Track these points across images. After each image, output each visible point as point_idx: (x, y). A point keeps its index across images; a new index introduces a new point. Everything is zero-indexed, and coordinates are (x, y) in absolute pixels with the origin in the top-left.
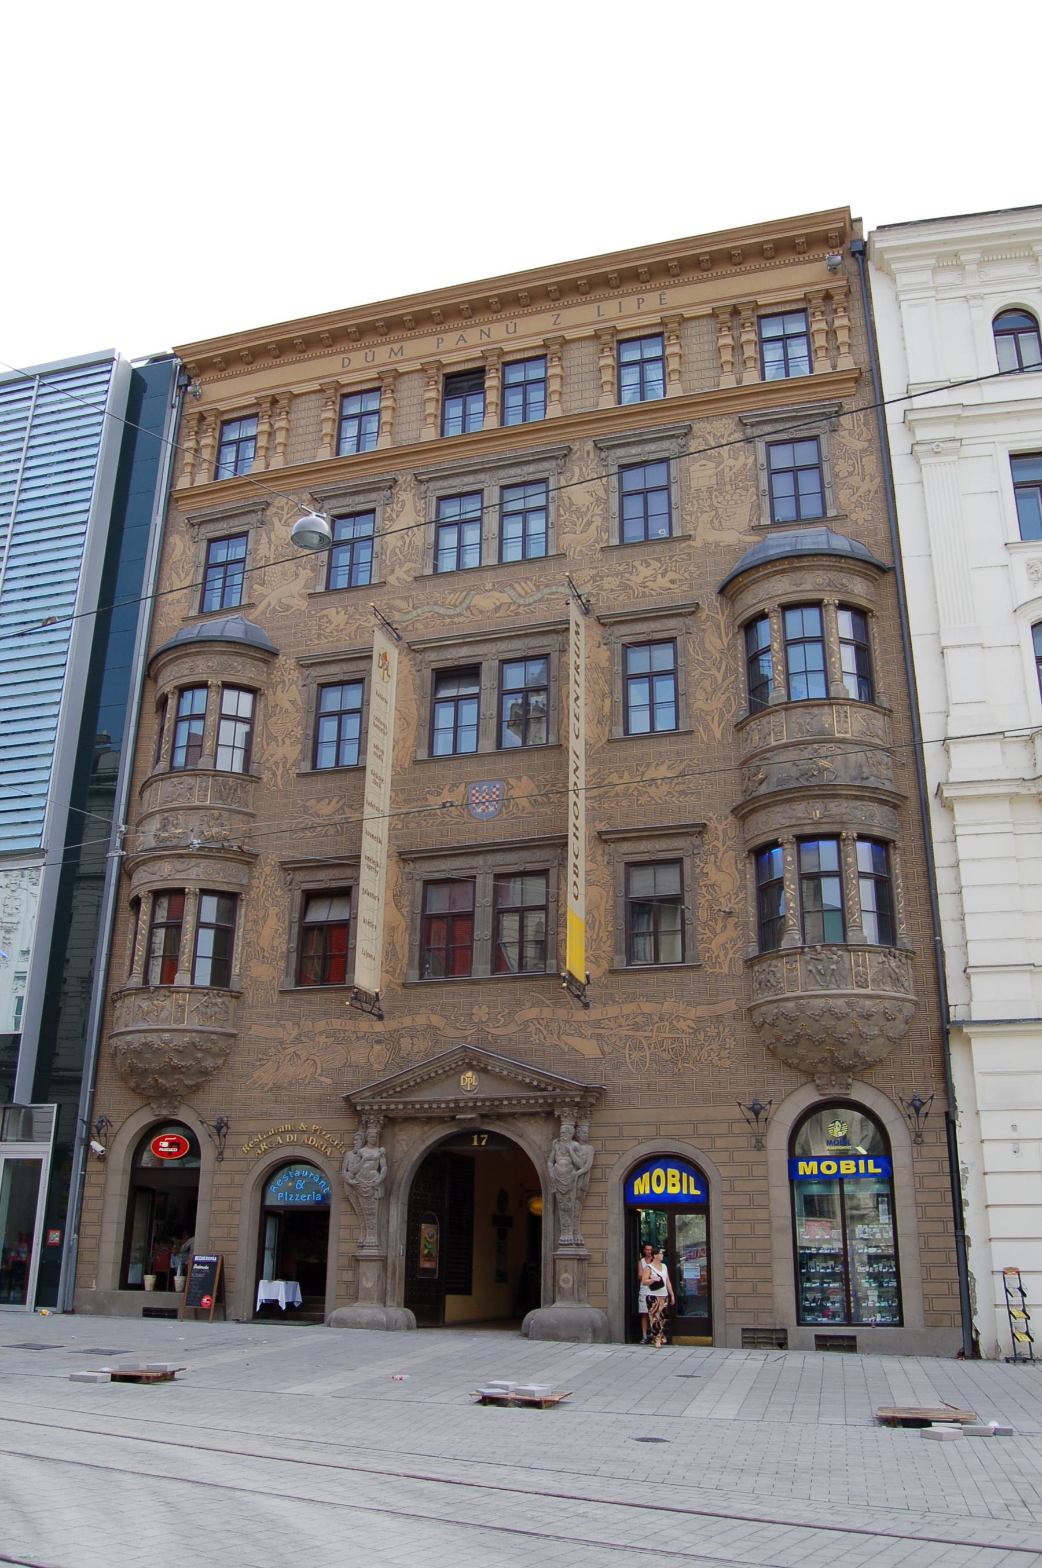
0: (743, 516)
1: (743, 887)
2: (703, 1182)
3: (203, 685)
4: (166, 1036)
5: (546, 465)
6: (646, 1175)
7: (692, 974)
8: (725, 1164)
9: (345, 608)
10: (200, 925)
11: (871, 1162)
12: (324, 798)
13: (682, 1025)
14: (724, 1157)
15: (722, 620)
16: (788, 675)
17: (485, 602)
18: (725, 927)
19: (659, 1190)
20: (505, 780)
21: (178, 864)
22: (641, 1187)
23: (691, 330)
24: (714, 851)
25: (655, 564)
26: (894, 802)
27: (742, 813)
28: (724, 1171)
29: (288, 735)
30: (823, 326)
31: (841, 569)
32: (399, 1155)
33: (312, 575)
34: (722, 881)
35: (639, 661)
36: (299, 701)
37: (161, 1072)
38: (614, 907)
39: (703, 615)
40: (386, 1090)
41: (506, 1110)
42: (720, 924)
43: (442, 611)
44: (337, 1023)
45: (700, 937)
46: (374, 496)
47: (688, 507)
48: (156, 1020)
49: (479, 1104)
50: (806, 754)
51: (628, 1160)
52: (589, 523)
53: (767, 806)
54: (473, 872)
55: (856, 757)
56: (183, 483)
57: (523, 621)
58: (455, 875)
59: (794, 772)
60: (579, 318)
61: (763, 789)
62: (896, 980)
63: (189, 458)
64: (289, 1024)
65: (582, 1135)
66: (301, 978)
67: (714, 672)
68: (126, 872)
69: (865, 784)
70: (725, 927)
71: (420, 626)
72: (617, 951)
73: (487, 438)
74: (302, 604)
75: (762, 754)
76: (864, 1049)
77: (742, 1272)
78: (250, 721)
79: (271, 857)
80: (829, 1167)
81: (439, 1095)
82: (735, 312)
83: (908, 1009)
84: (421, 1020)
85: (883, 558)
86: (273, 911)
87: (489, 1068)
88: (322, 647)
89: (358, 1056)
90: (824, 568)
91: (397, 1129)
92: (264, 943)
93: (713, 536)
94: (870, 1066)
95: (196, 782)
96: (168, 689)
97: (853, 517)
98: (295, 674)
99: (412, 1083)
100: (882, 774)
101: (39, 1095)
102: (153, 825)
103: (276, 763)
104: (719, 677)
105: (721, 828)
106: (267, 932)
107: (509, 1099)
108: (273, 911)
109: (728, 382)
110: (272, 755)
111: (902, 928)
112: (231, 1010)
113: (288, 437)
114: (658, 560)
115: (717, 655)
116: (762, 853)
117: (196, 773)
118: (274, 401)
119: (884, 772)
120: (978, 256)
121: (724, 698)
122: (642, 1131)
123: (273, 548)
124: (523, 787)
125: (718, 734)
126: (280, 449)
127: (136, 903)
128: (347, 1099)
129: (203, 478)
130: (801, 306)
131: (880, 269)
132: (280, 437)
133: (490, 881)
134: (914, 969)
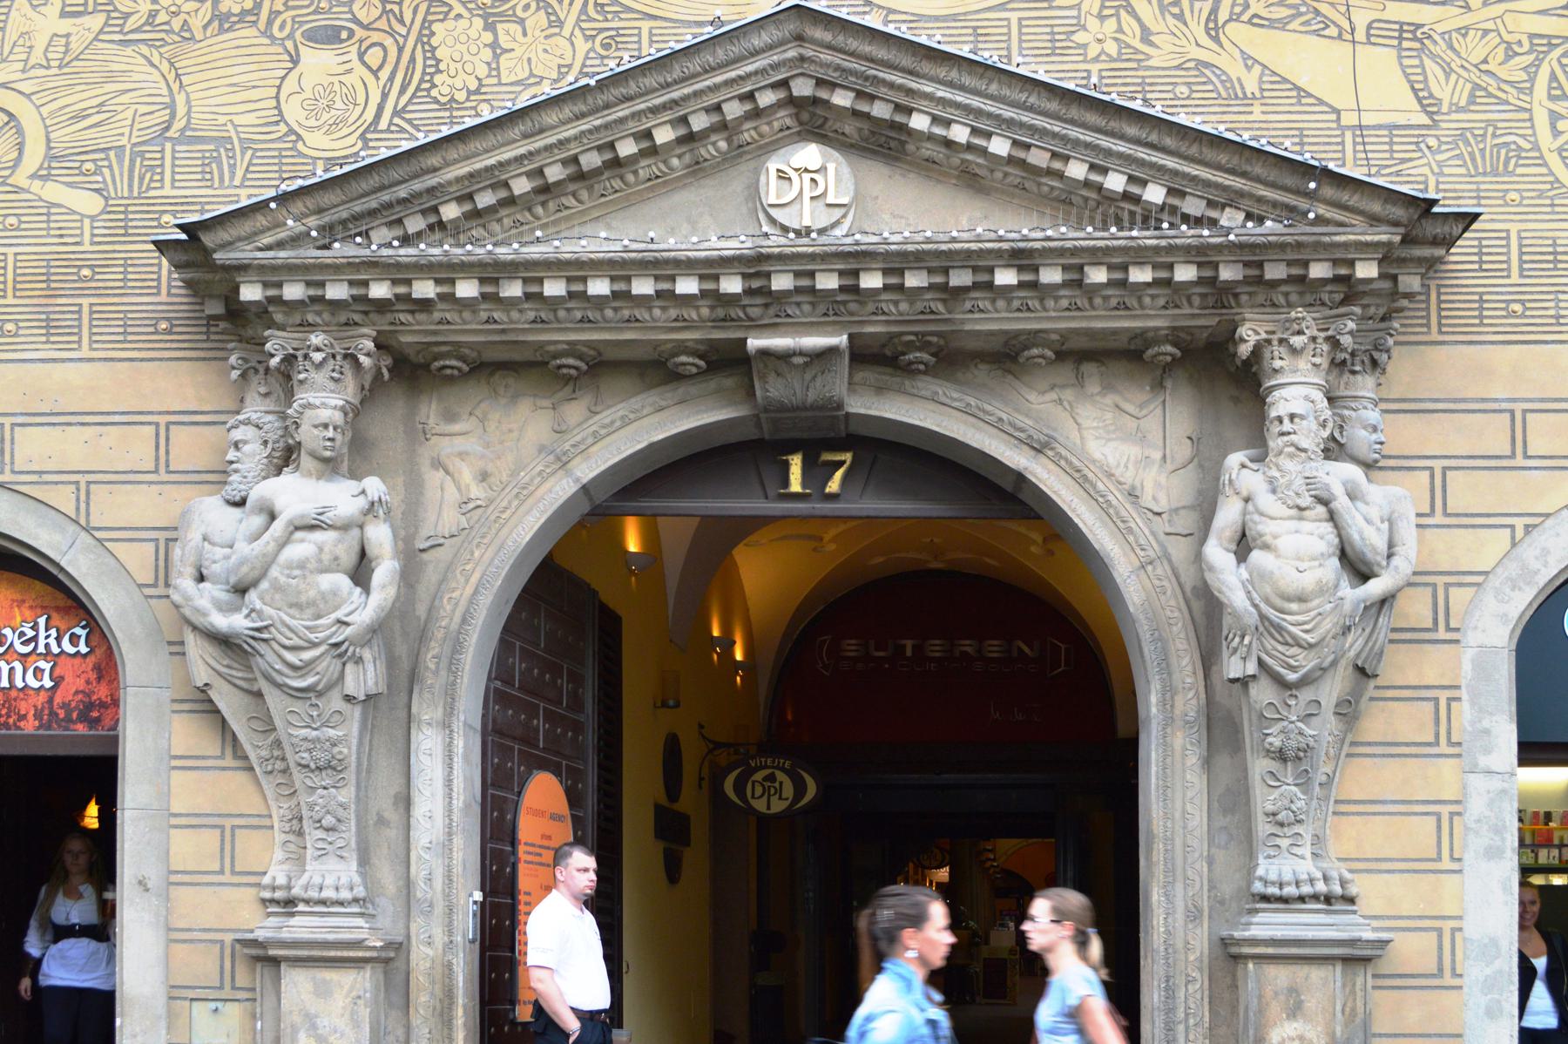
49: (872, 281)
87: (919, 122)
91: (430, 411)
99: (521, 186)
107: (1022, 258)
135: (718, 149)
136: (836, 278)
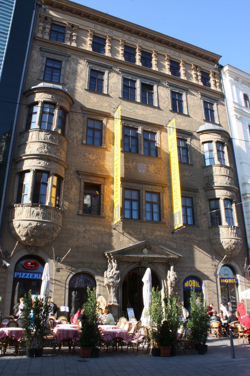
10: (53, 186)
12: (91, 154)
18: (204, 217)
24: (200, 197)
33: (85, 83)
36: (81, 120)
42: (202, 217)
44: (98, 228)
45: (198, 219)
64: (81, 226)
70: (204, 217)
103: (73, 138)
108: (74, 187)
110: (72, 135)
123: (71, 70)
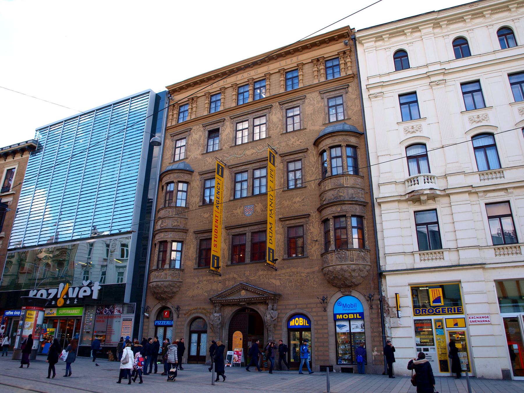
0: (320, 121)
1: (320, 233)
2: (309, 322)
3: (172, 182)
4: (162, 283)
5: (266, 111)
6: (293, 320)
7: (306, 259)
8: (315, 316)
9: (211, 157)
11: (358, 315)
13: (303, 275)
14: (315, 314)
15: (315, 152)
16: (331, 168)
17: (248, 152)
19: (297, 324)
20: (254, 205)
21: (166, 234)
22: (292, 323)
23: (306, 67)
25: (296, 138)
26: (364, 205)
27: (320, 210)
28: (315, 318)
29: (196, 195)
30: (343, 62)
31: (346, 135)
32: (225, 315)
34: (314, 230)
35: (292, 166)
37: (161, 293)
38: (284, 240)
39: (309, 152)
40: (221, 296)
41: (254, 301)
43: (237, 156)
44: (209, 278)
46: (219, 124)
47: (305, 120)
48: (158, 279)
50: (336, 191)
51: (288, 315)
52: (277, 127)
53: (325, 208)
54: (245, 232)
55: (351, 191)
56: (169, 125)
57: (259, 157)
58: (241, 233)
59: (333, 197)
60: (274, 66)
61: (325, 203)
62: (364, 259)
63: (170, 117)
64: (196, 278)
65: (274, 308)
66: (199, 265)
67: (312, 168)
68: (154, 236)
69: (354, 199)
71: (231, 161)
72: (285, 254)
73: (249, 104)
74: (200, 157)
75: (325, 191)
76: (354, 280)
77: (320, 349)
78: (186, 192)
79: (191, 230)
80: (346, 316)
81: (235, 297)
82: (318, 60)
83: (368, 268)
84: (231, 276)
85: (360, 130)
86: (192, 246)
88: (205, 169)
89: (214, 287)
90: (342, 135)
92: (190, 255)
93: (312, 128)
94: (357, 285)
95: (170, 210)
96: (163, 184)
97: (352, 118)
98: (198, 177)
100: (361, 197)
101: (131, 301)
102: (160, 223)
104: (314, 170)
105: (314, 215)
106: (190, 252)
108: (192, 246)
109: (316, 81)
111: (367, 243)
112: (181, 275)
113: (196, 109)
114: (296, 136)
115: (313, 163)
116: (325, 221)
117: (170, 207)
118: (193, 99)
119: (360, 195)
120: (388, 36)
121: (315, 176)
122: (292, 307)
124: (259, 207)
125: (313, 187)
126: (194, 113)
127: (155, 245)
128: (210, 299)
129: (174, 123)
130: (337, 56)
131: (359, 43)
132: (194, 109)
133: (250, 234)
134: (370, 255)
135: (239, 291)
136: (244, 300)
